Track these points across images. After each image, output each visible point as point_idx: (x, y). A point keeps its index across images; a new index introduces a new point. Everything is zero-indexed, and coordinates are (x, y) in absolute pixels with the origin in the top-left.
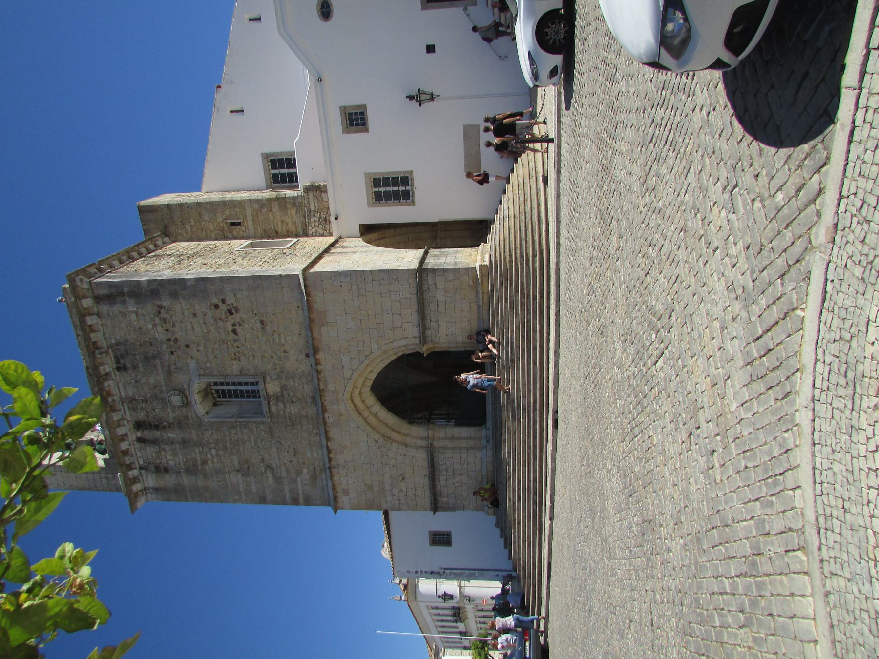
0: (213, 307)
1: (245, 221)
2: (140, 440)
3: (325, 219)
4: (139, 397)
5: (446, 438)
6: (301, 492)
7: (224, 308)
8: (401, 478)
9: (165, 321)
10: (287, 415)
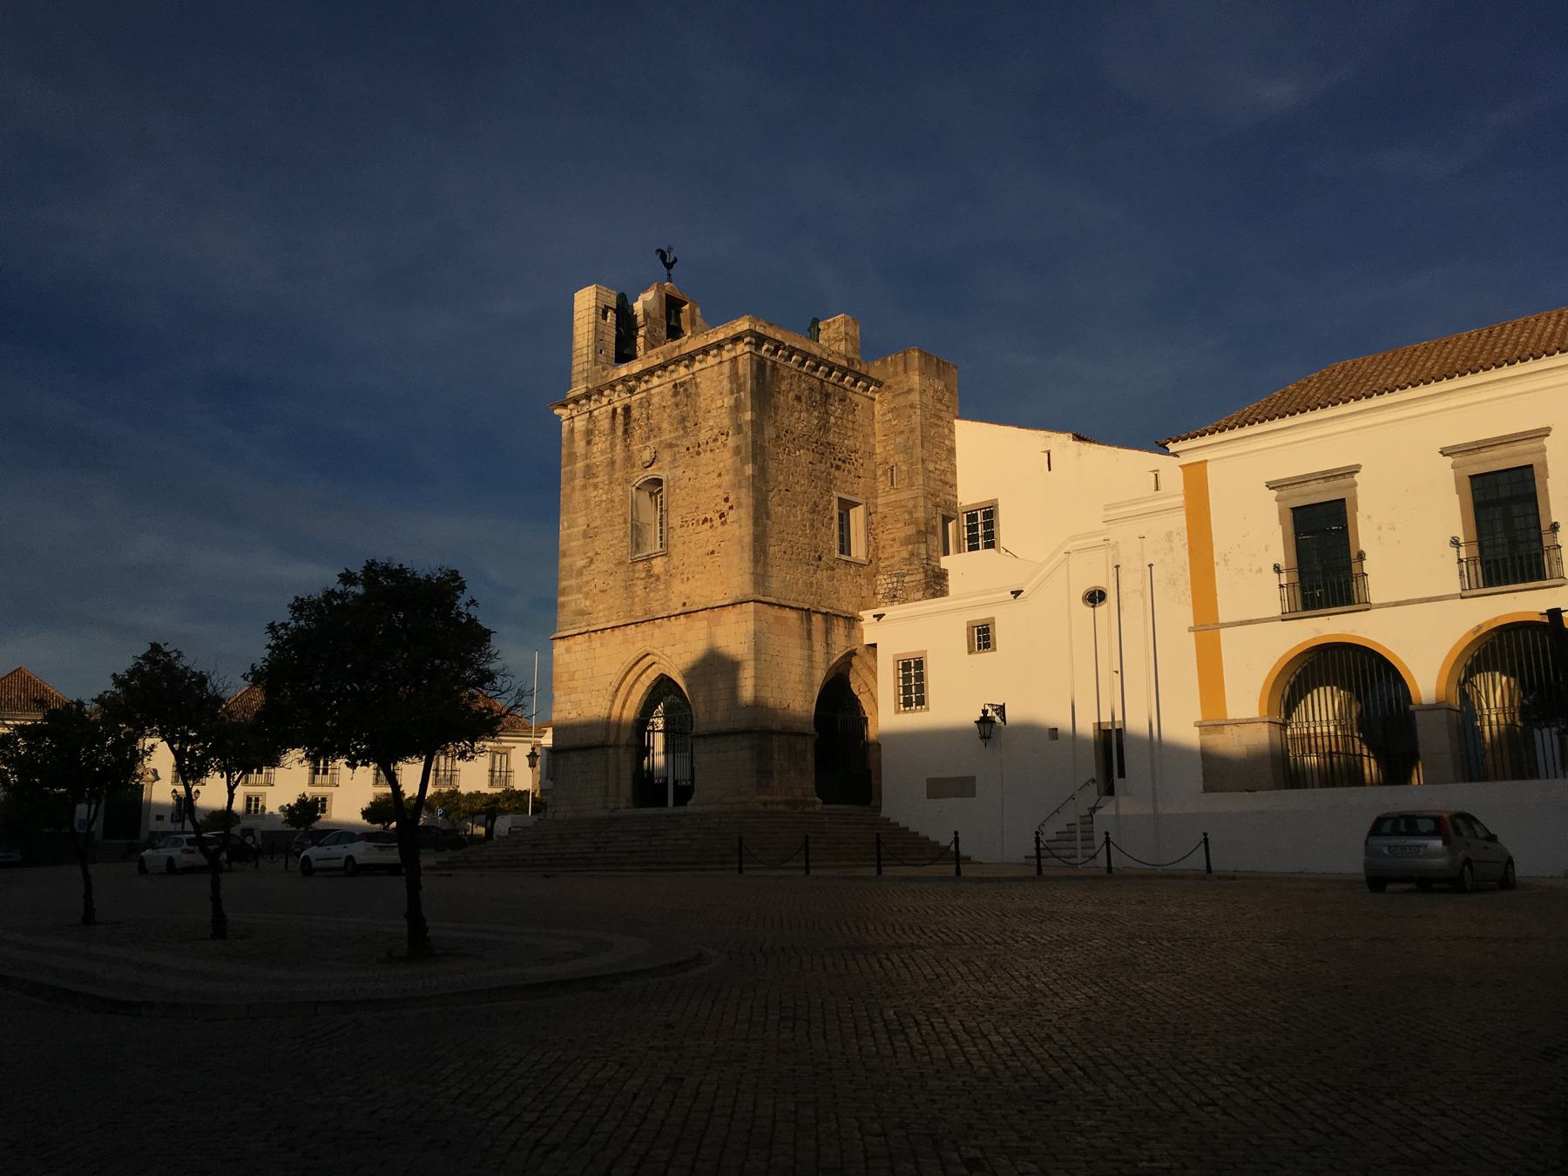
2: (615, 410)
3: (895, 596)
6: (570, 598)
7: (724, 507)
8: (580, 712)
9: (715, 440)
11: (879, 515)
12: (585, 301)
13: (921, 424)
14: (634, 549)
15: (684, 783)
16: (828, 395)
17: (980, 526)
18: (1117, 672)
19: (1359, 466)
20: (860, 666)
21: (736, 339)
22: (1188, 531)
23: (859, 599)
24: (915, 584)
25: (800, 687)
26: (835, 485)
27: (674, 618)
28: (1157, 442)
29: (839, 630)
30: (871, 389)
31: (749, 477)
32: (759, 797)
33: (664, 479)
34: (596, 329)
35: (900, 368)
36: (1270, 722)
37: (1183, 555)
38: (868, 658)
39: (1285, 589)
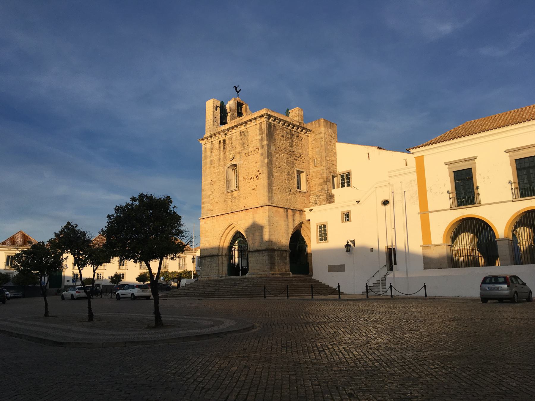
0: (258, 170)
1: (316, 167)
2: (220, 141)
3: (316, 203)
5: (222, 261)
6: (206, 205)
7: (258, 174)
8: (209, 244)
9: (254, 151)
10: (228, 199)
11: (311, 176)
12: (210, 105)
13: (325, 145)
14: (227, 189)
15: (245, 268)
16: (293, 135)
17: (345, 179)
18: (393, 228)
19: (477, 157)
20: (305, 227)
21: (261, 116)
22: (417, 180)
23: (304, 204)
24: (323, 199)
25: (284, 235)
26: (296, 166)
27: (241, 211)
28: (406, 149)
29: (297, 215)
30: (308, 132)
31: (266, 163)
32: (271, 272)
33: (237, 164)
34: (214, 114)
35: (317, 125)
36: (446, 245)
37: (416, 188)
38: (307, 224)
39: (451, 199)
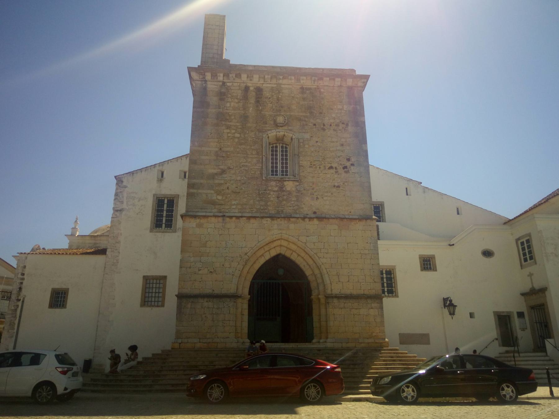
4: (281, 96)
6: (200, 191)
7: (348, 164)
8: (212, 270)
10: (268, 192)
